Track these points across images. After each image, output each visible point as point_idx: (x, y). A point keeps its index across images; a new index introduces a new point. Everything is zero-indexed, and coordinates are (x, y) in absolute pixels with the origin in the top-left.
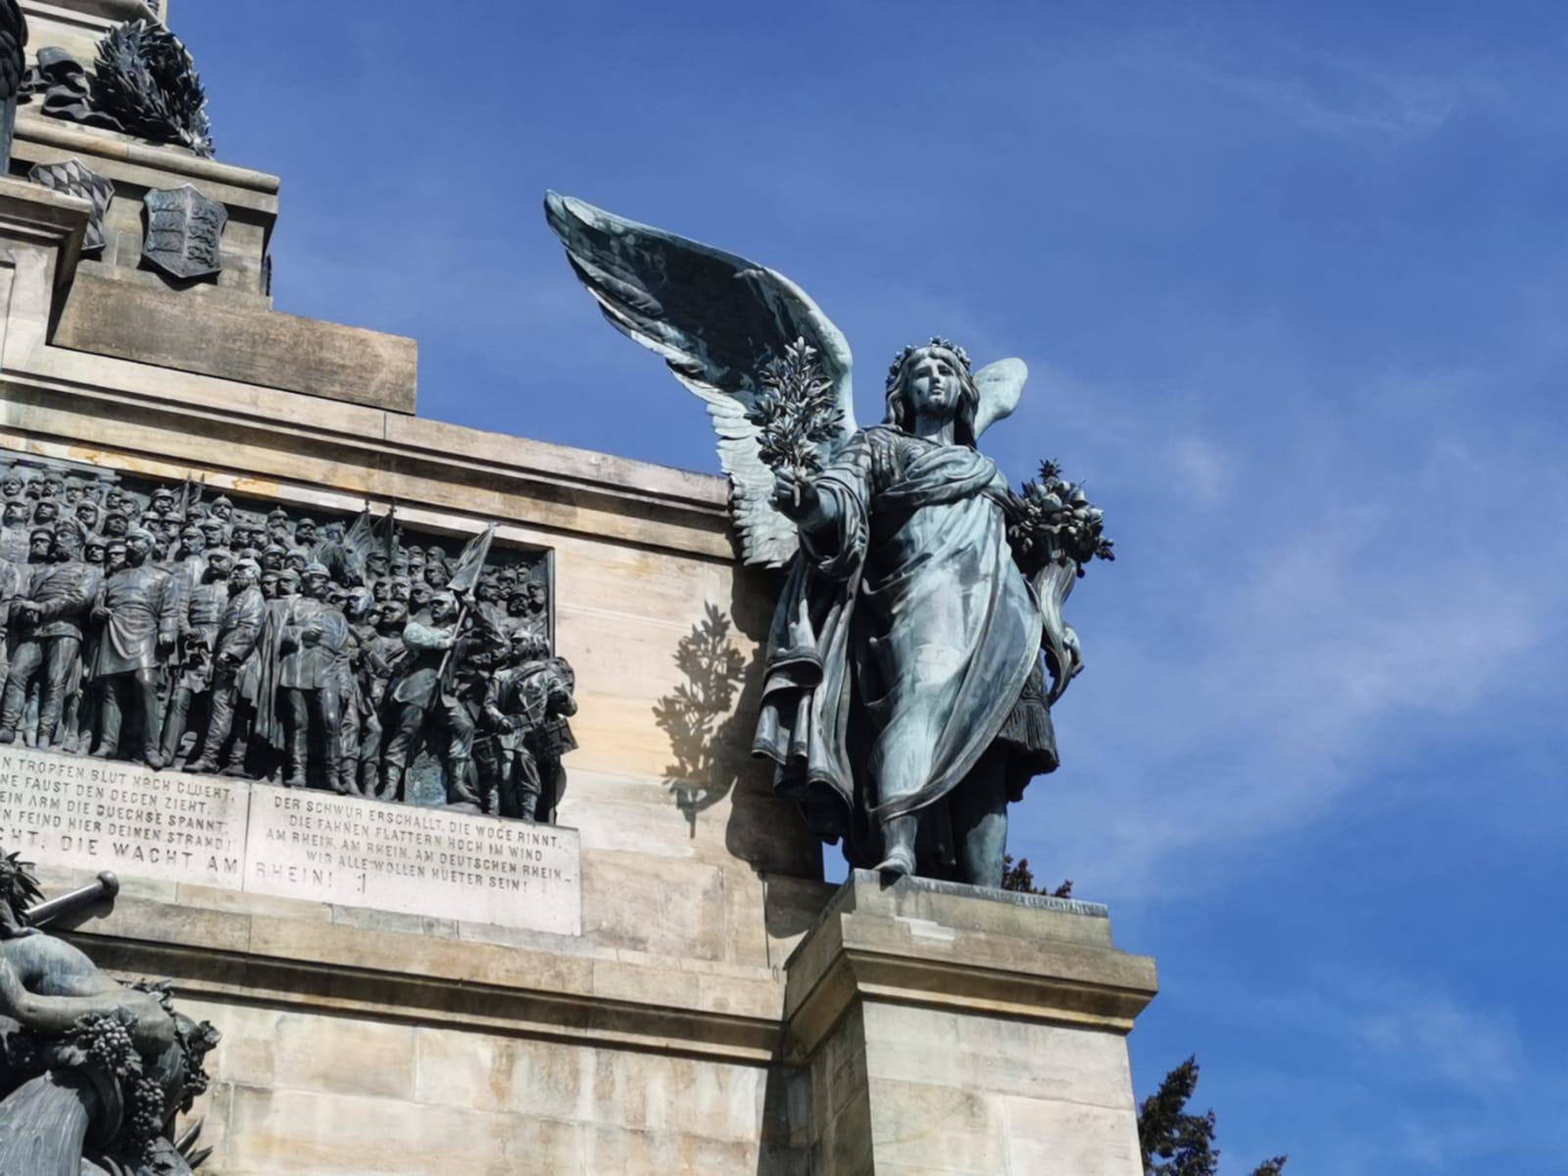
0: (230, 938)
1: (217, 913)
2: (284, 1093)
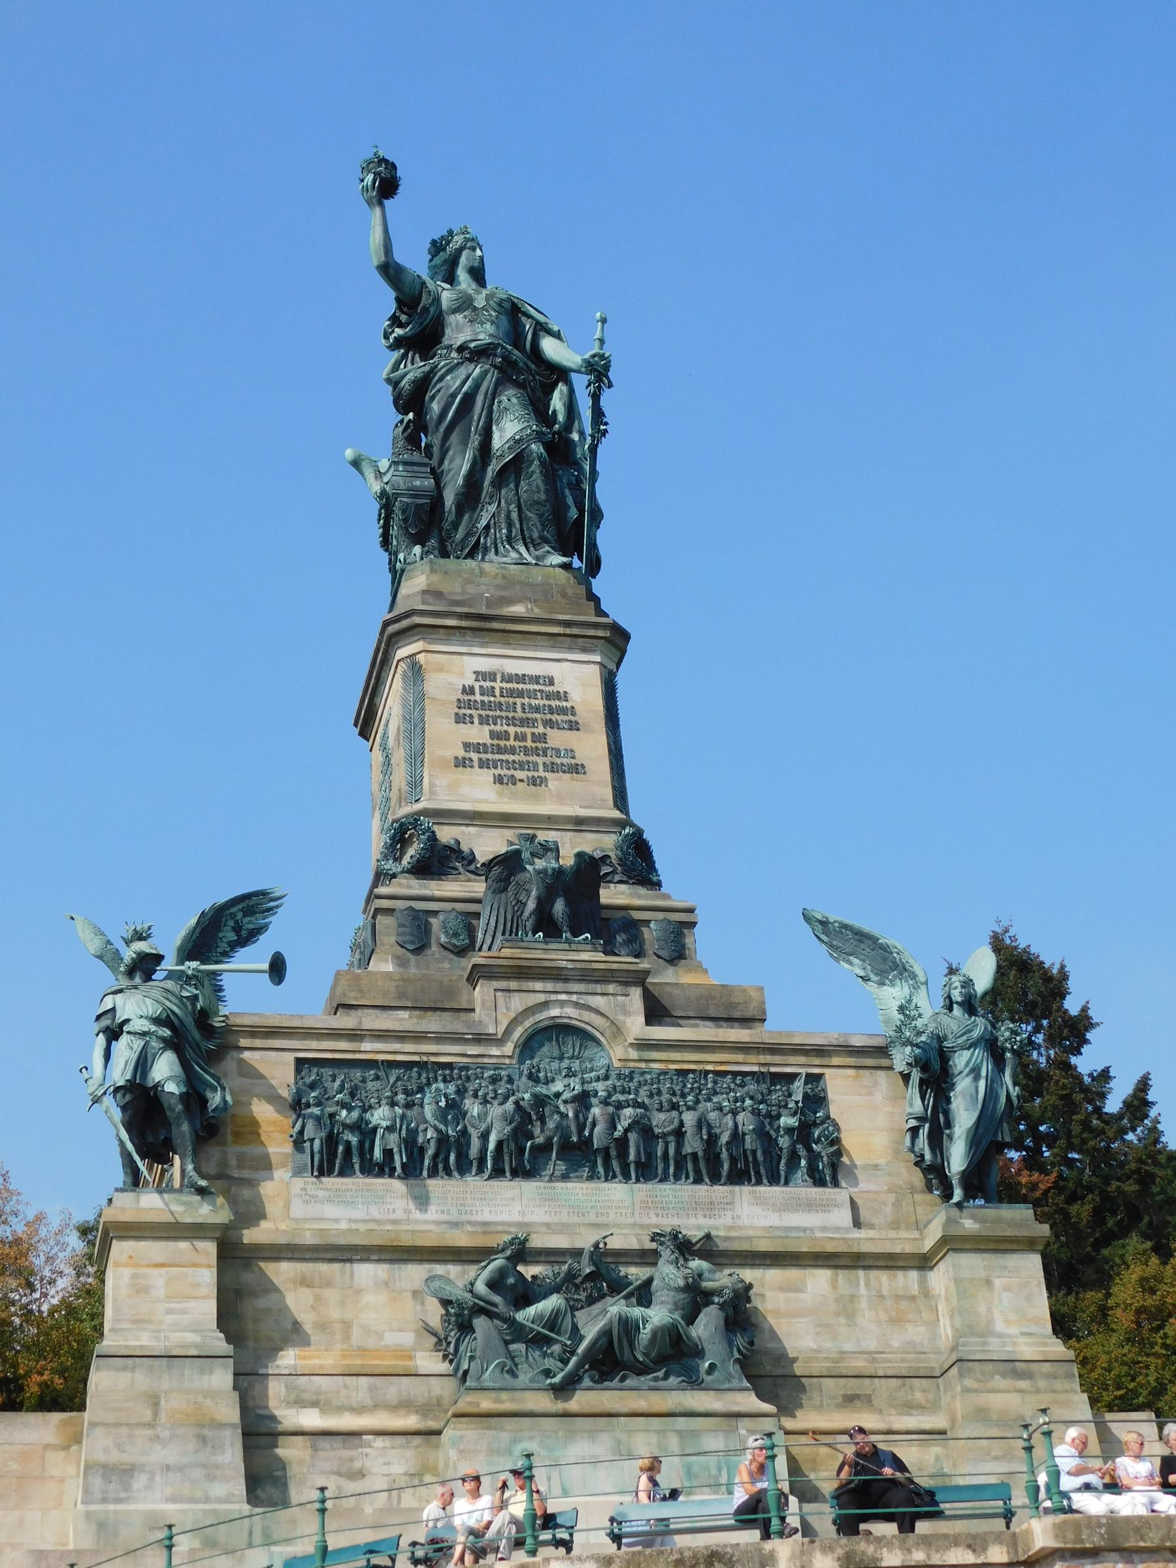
0: (745, 1246)
2: (769, 1294)
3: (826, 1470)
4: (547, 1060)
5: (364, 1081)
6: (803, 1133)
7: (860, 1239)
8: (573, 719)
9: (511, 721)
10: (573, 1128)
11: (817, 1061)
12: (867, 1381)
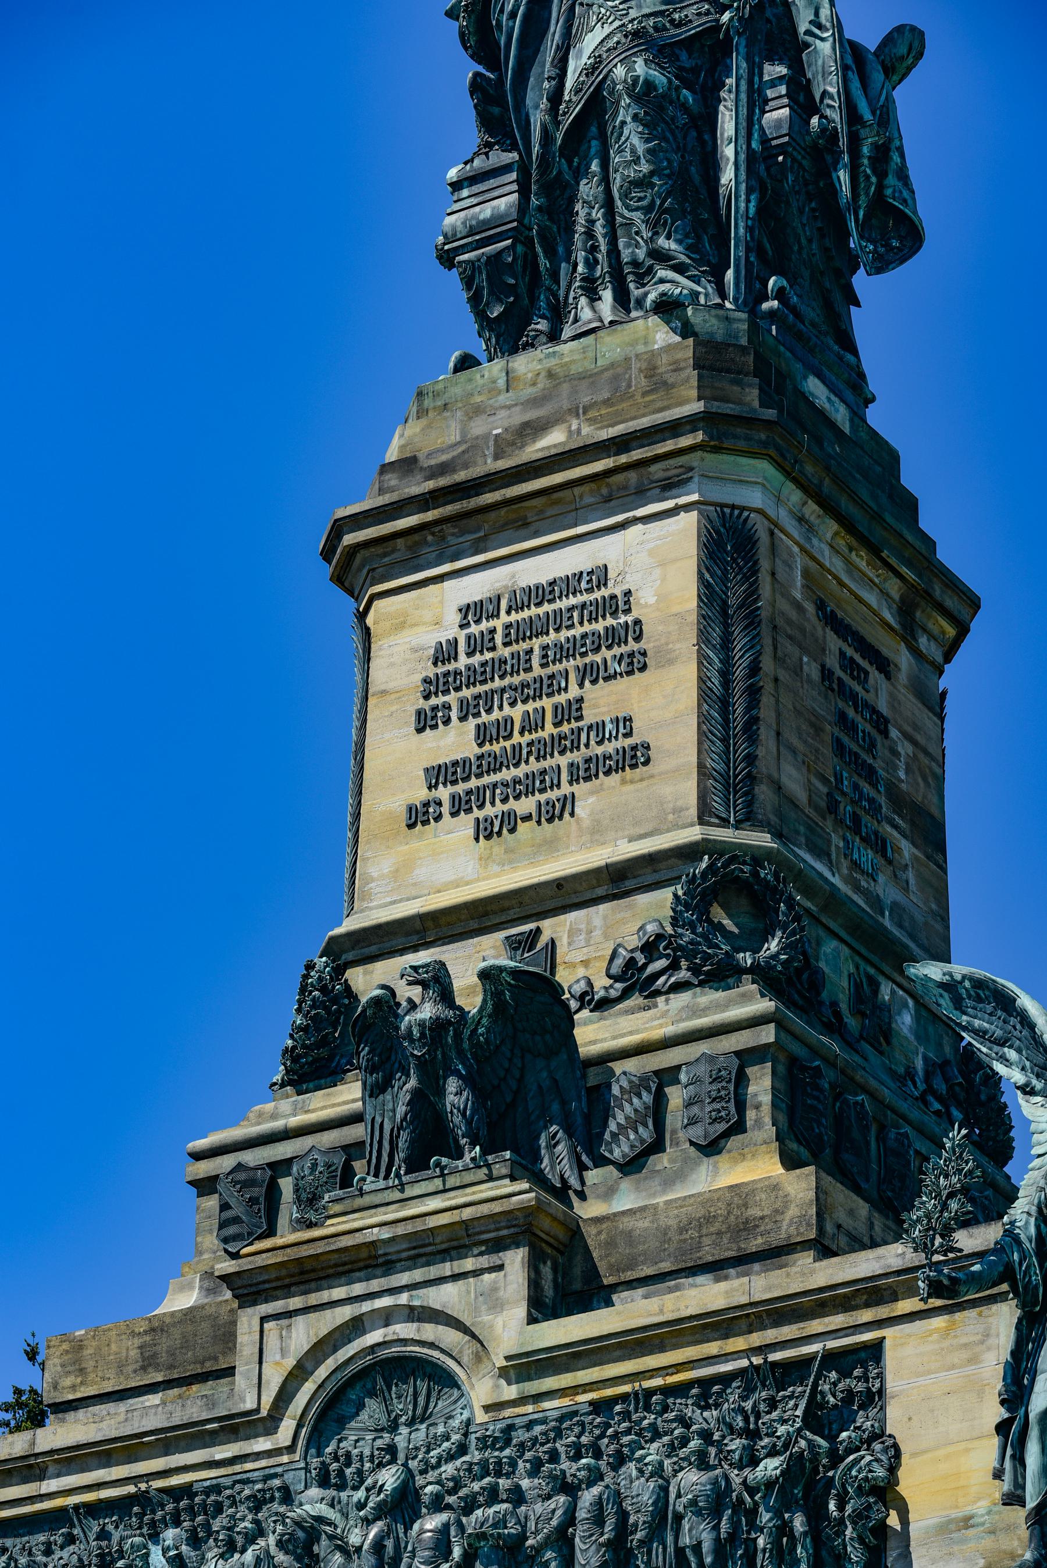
4: (369, 1437)
8: (632, 646)
9: (522, 693)
11: (866, 1315)
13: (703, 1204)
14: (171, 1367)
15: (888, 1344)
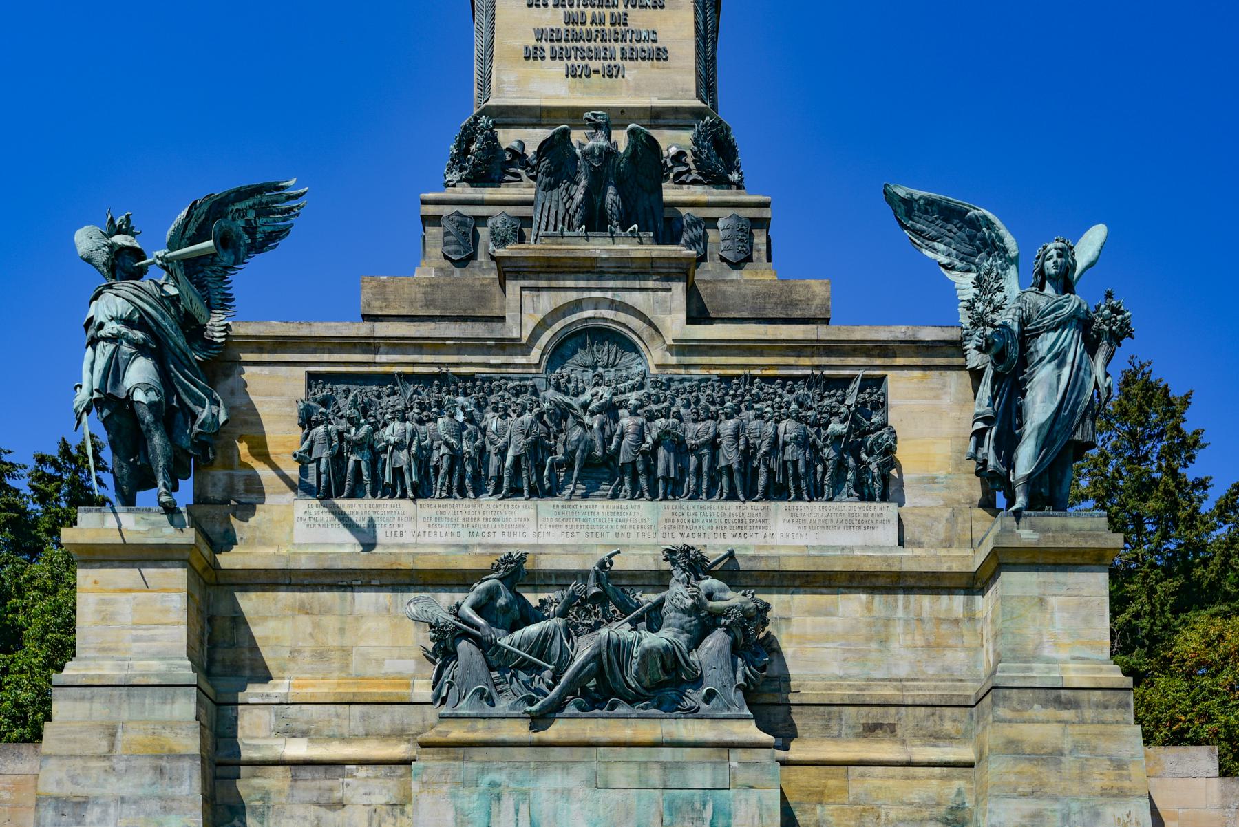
0: (773, 566)
1: (767, 557)
3: (834, 803)
5: (379, 397)
6: (850, 445)
7: (901, 557)
10: (598, 442)
11: (879, 361)
12: (892, 710)
13: (767, 286)
14: (445, 309)
15: (889, 378)
